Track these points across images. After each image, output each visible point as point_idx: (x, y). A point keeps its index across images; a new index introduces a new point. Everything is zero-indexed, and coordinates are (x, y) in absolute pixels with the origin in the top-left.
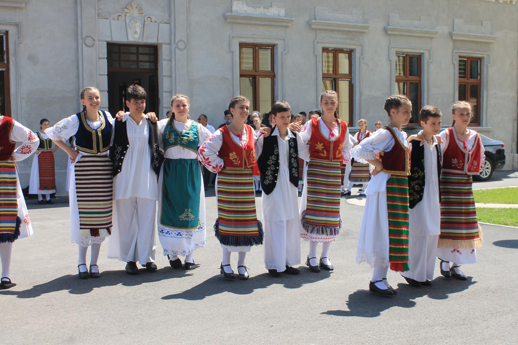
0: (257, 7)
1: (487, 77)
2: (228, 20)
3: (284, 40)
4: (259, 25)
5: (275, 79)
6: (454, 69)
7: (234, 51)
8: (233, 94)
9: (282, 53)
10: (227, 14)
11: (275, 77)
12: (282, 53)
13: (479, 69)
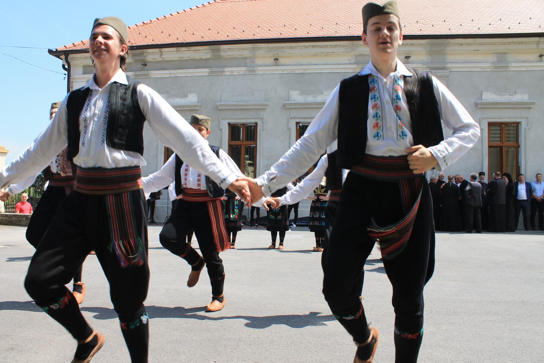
0: (503, 95)
2: (479, 106)
3: (527, 118)
4: (505, 108)
5: (519, 148)
7: (483, 128)
8: (483, 160)
9: (525, 128)
10: (478, 102)
11: (519, 147)
12: (525, 128)
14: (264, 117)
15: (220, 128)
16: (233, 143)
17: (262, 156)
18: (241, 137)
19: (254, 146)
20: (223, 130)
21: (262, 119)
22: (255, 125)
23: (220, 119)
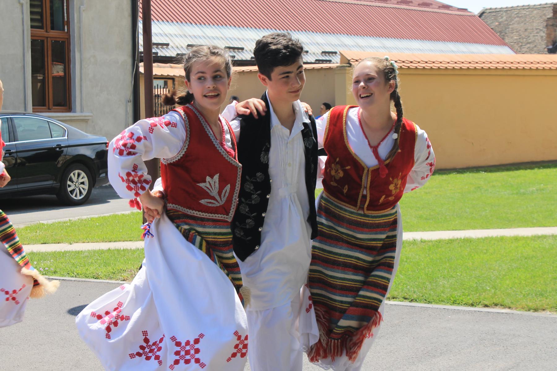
1: (80, 28)
6: (23, 13)
13: (65, 15)
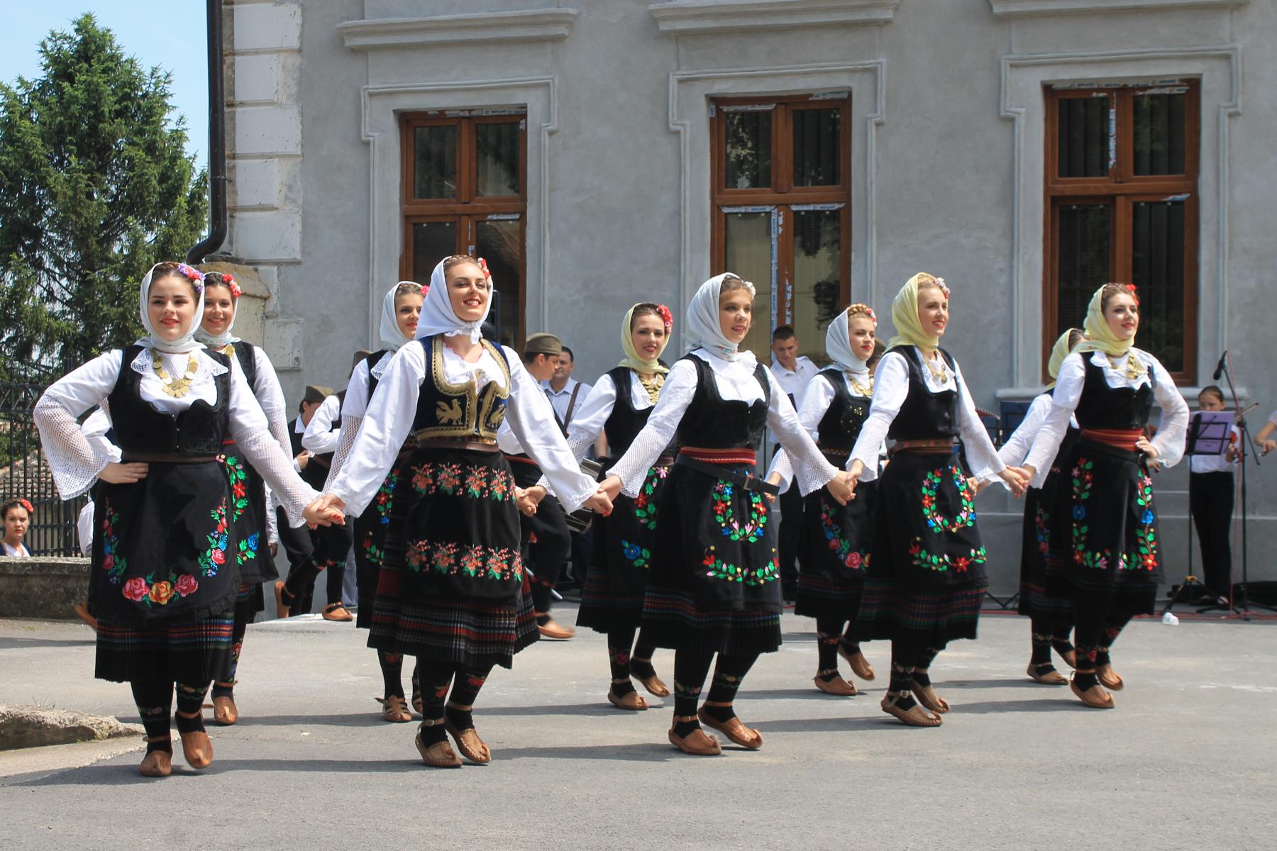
14: (1240, 46)
15: (1003, 113)
16: (1073, 186)
17: (1231, 248)
18: (1112, 155)
19: (1181, 203)
20: (1021, 121)
21: (1227, 57)
22: (1183, 90)
23: (1005, 67)
